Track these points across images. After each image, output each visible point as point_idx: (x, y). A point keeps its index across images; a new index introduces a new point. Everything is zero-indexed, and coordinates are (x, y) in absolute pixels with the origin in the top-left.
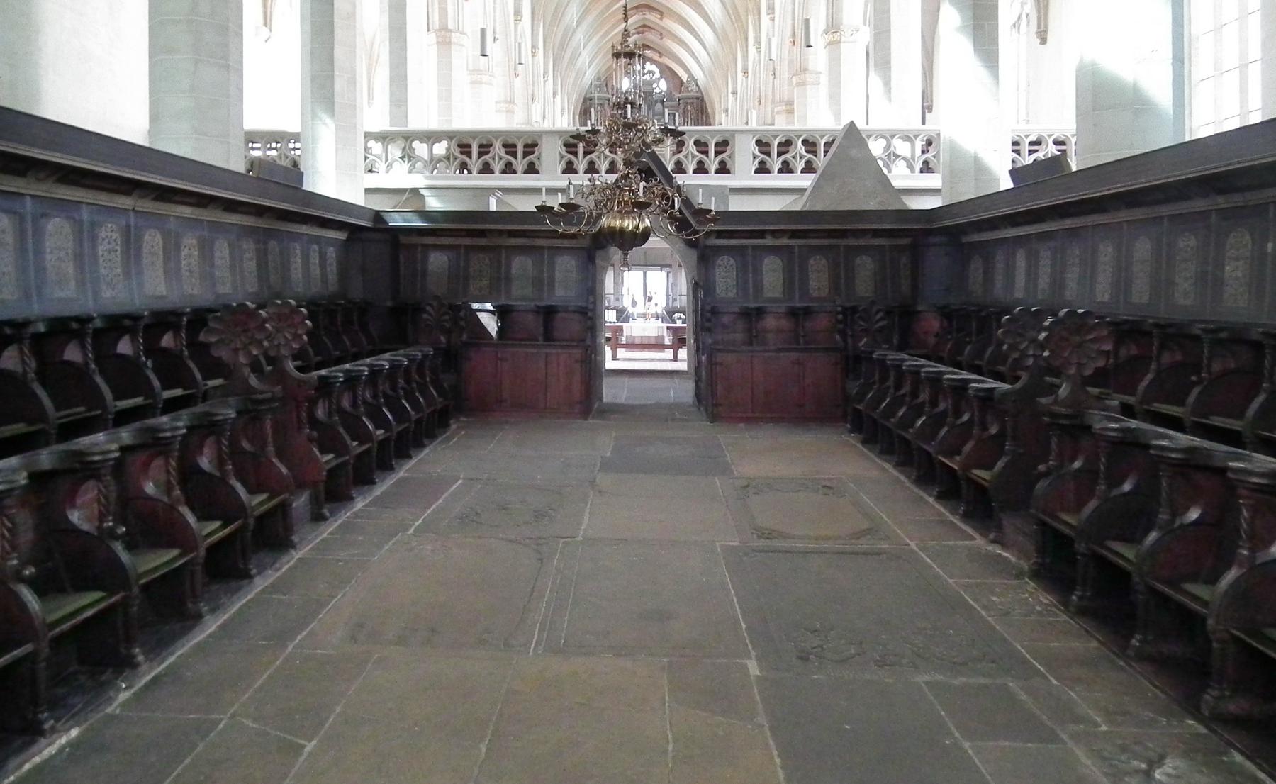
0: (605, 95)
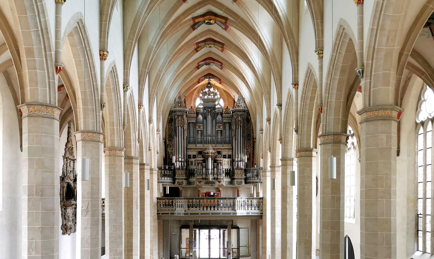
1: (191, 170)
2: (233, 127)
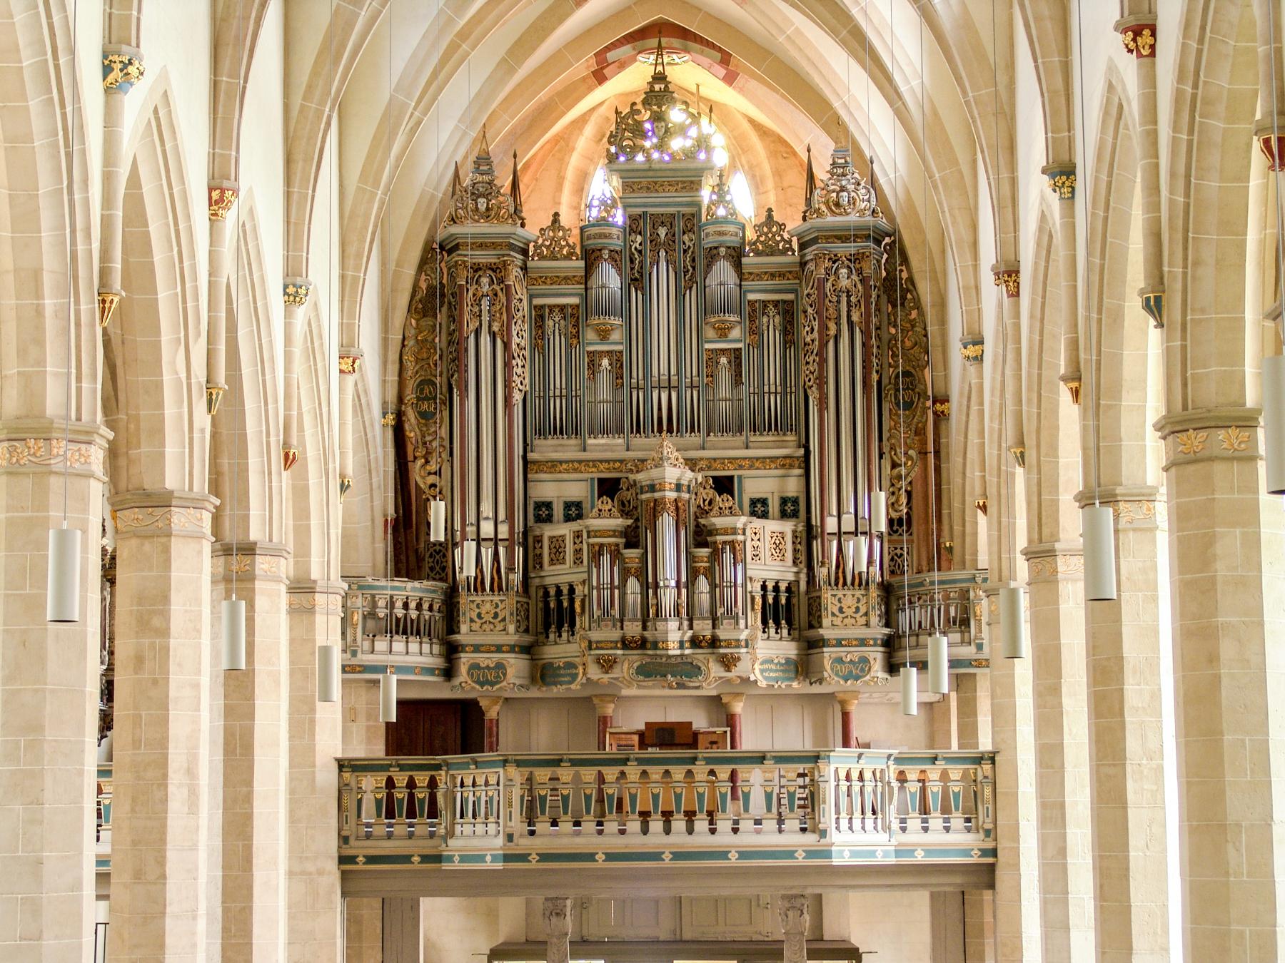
0: (505, 229)
1: (552, 592)
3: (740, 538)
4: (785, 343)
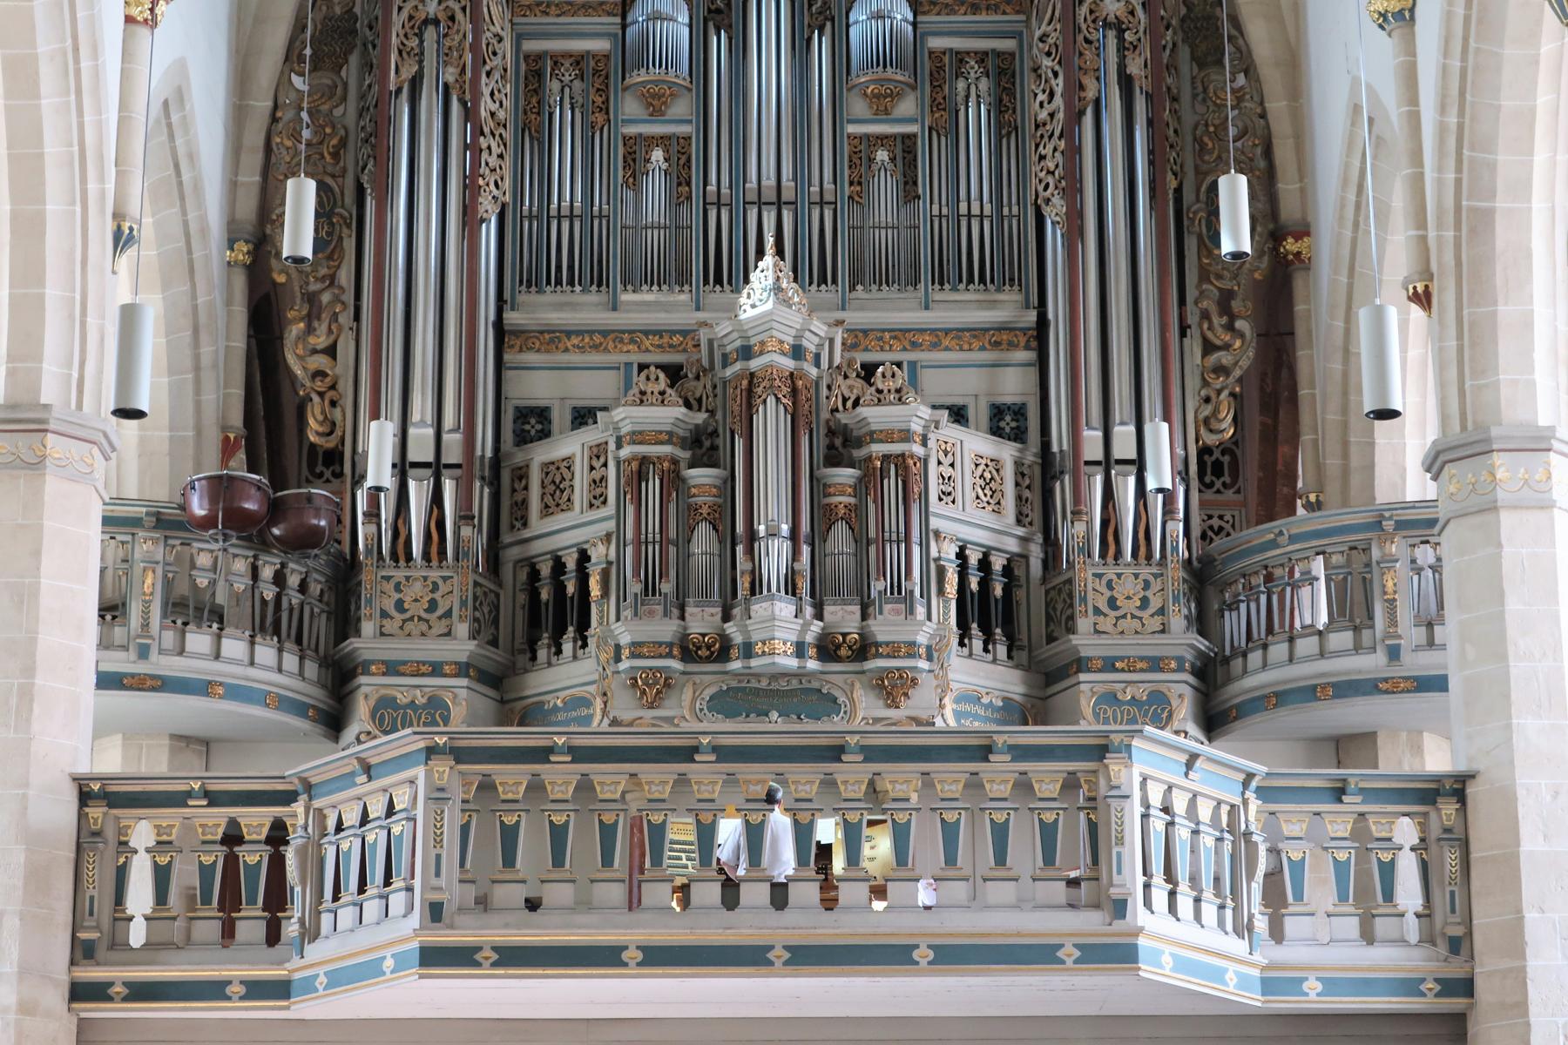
1: (545, 569)
2: (1041, 97)
3: (918, 449)
4: (1000, 126)
